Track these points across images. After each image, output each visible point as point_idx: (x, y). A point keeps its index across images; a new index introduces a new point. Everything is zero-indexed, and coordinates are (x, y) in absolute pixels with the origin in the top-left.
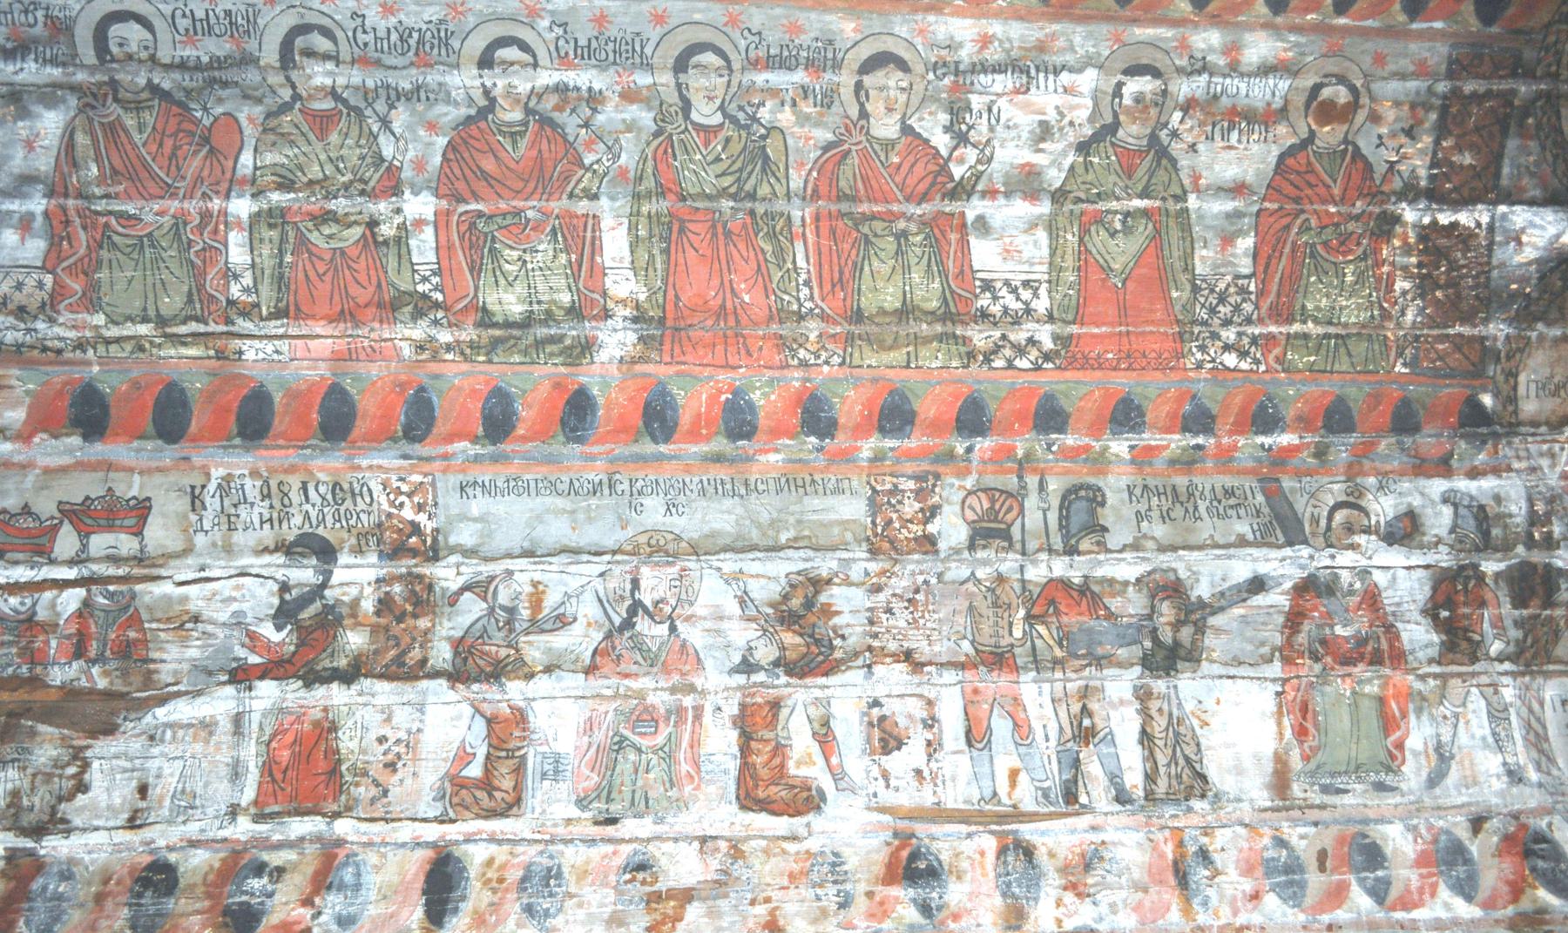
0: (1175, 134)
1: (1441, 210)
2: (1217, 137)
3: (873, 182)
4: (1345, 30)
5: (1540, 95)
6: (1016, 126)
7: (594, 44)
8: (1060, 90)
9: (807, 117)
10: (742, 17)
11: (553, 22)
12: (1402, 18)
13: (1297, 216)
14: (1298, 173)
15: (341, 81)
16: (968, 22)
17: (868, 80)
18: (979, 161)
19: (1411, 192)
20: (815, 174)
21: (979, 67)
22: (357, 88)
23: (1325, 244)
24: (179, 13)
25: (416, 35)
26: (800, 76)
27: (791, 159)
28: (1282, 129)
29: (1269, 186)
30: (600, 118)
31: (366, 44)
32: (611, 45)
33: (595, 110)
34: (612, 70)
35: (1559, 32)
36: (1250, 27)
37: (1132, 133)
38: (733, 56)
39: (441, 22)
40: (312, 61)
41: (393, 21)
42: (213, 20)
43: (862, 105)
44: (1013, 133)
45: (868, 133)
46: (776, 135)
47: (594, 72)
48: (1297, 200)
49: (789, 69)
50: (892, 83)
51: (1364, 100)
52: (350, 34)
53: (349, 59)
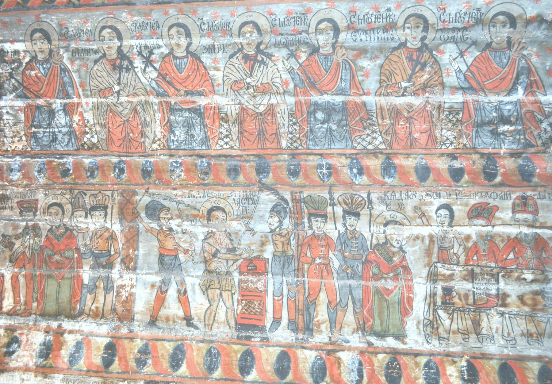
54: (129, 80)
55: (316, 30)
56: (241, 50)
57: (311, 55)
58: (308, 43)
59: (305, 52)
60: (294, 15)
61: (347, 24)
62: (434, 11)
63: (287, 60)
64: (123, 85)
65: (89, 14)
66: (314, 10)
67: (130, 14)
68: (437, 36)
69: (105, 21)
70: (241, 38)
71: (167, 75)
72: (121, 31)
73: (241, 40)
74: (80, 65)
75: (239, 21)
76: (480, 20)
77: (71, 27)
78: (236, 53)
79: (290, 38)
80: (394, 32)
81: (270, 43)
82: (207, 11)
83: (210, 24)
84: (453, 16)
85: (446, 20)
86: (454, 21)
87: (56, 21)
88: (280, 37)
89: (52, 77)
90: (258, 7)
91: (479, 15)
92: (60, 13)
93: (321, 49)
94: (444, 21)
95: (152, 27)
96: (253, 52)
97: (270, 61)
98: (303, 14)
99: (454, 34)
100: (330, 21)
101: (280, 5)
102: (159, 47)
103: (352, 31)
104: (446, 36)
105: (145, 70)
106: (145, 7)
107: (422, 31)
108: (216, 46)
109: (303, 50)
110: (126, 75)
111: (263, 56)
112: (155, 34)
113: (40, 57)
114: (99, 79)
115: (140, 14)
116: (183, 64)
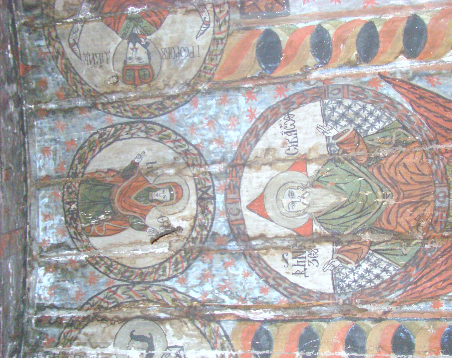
4: (364, 12)
35: (221, 33)
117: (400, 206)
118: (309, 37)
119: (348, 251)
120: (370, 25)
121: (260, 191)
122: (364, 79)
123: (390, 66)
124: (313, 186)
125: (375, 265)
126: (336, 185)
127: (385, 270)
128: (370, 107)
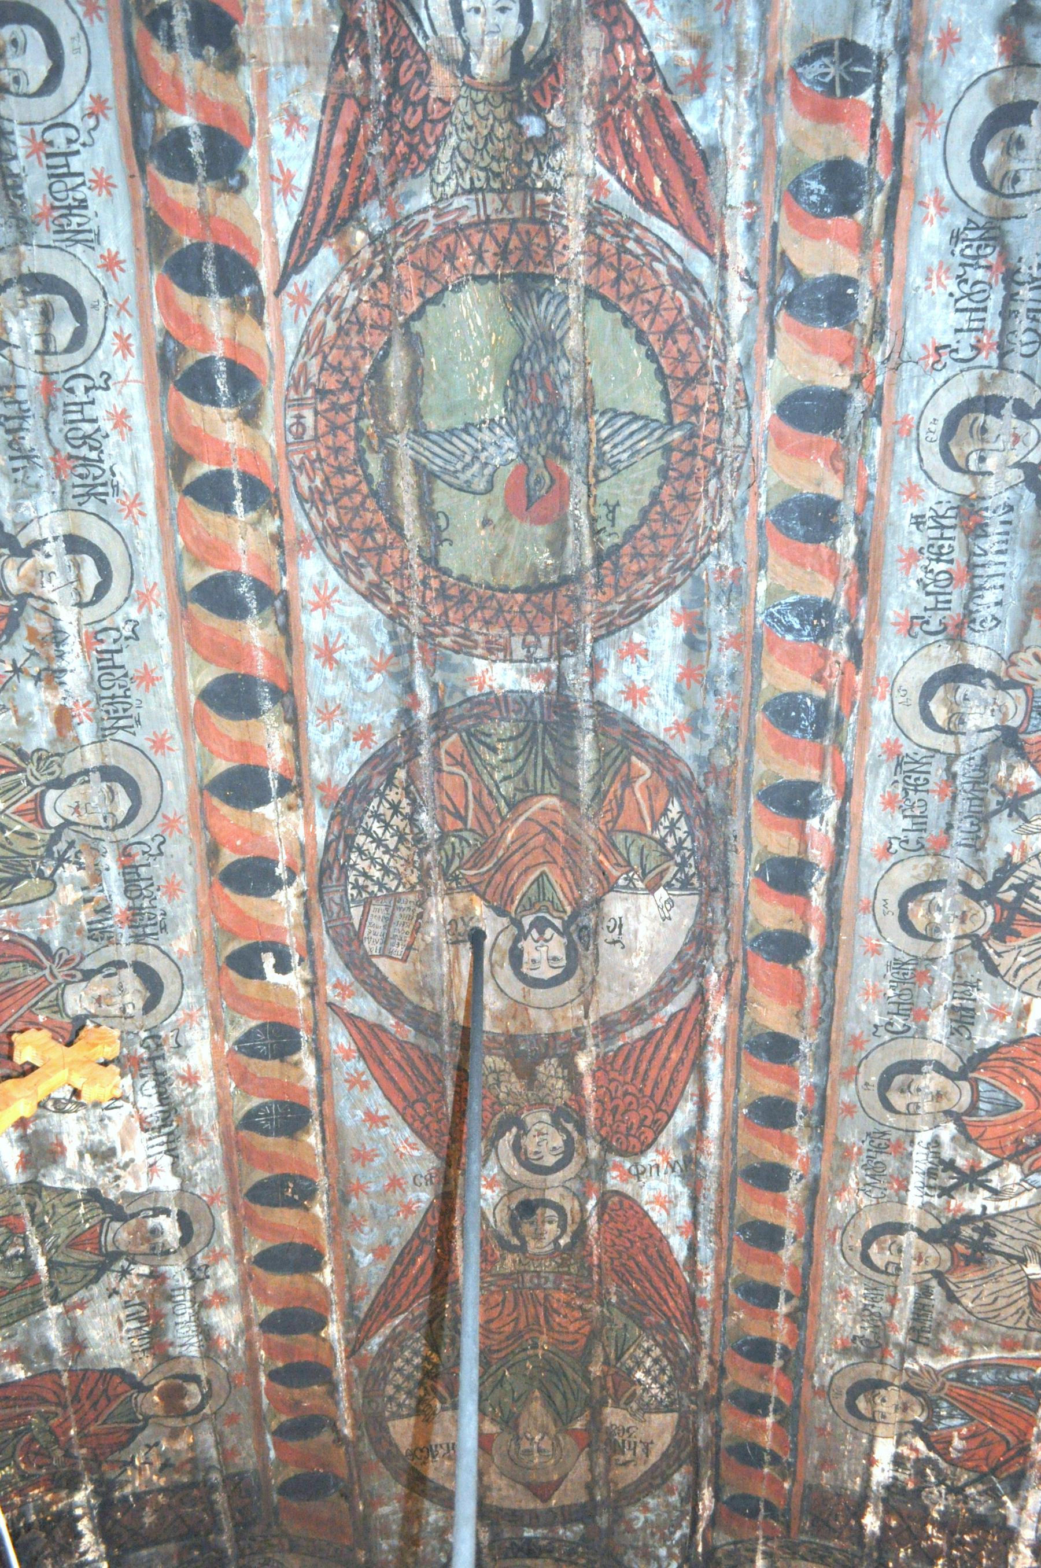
0: (124, 1273)
1: (91, 1519)
2: (129, 1311)
3: (10, 1001)
4: (256, 1383)
5: (222, 1552)
6: (105, 1127)
7: (118, 673)
8: (151, 1161)
9: (74, 917)
10: (176, 834)
11: (137, 623)
12: (274, 1425)
13: (57, 1405)
14: (105, 1391)
15: (19, 356)
16: (208, 1060)
17: (128, 973)
18: (56, 1101)
19: (104, 1489)
20: (6, 937)
21: (162, 1079)
22: (13, 375)
23: (33, 1440)
24: (72, 134)
25: (94, 455)
26: (120, 903)
27: (21, 908)
28: (148, 1362)
29: (86, 1371)
30: (28, 686)
31: (71, 390)
32: (121, 692)
33: (37, 679)
34: (90, 696)
36: (244, 1305)
37: (120, 1234)
38: (130, 829)
39: (116, 487)
40: (38, 317)
41: (107, 426)
42: (71, 182)
43: (99, 971)
44: (96, 1126)
45: (67, 983)
46: (47, 886)
47: (85, 675)
48: (76, 1398)
49: (126, 891)
50: (128, 998)
51: (190, 1420)
52: (81, 370)
53: (49, 368)
54: (1017, 1235)
55: (949, 732)
56: (977, 942)
57: (1023, 754)
58: (985, 759)
59: (1011, 768)
60: (899, 791)
61: (943, 644)
62: (940, 382)
63: (1027, 821)
64: (1029, 1252)
65: (826, 1283)
66: (892, 734)
67: (838, 1193)
68: (1020, 367)
69: (847, 1251)
70: (943, 935)
71: (1018, 1141)
72: (879, 1222)
73: (949, 938)
74: (954, 1335)
75: (896, 935)
76: (988, 230)
77: (853, 1328)
78: (984, 956)
79: (963, 805)
80: (988, 503)
81: (969, 861)
82: (858, 1011)
83: (893, 1008)
84: (962, 320)
85: (973, 341)
86: (981, 315)
87: (834, 1356)
88: (955, 832)
89: (977, 1407)
90: (864, 883)
91: (971, 235)
92: (816, 1341)
93: (1009, 723)
94: (977, 348)
95: (879, 1150)
96: (990, 910)
97: (1025, 867)
98: (899, 764)
99: (1022, 310)
100: (928, 691)
101: (865, 824)
102: (936, 1142)
103: (967, 631)
104: (1025, 338)
105: (995, 1192)
106: (826, 1155)
107: (999, 416)
108: (956, 1002)
109: (1002, 773)
110: (1000, 1238)
111: (1005, 886)
112: (899, 1145)
113: (918, 1415)
114: (1001, 1302)
115: (841, 1170)
116: (994, 1095)
117: (550, 1329)
118: (290, 1444)
119: (616, 1391)
120: (274, 1376)
121: (519, 1487)
122: (356, 1372)
123: (336, 1345)
124: (516, 1427)
125: (639, 1364)
126: (515, 1401)
127: (647, 1352)
128: (399, 1363)
